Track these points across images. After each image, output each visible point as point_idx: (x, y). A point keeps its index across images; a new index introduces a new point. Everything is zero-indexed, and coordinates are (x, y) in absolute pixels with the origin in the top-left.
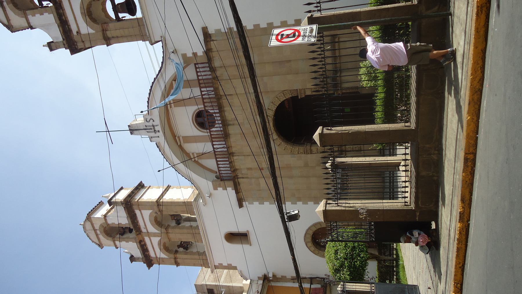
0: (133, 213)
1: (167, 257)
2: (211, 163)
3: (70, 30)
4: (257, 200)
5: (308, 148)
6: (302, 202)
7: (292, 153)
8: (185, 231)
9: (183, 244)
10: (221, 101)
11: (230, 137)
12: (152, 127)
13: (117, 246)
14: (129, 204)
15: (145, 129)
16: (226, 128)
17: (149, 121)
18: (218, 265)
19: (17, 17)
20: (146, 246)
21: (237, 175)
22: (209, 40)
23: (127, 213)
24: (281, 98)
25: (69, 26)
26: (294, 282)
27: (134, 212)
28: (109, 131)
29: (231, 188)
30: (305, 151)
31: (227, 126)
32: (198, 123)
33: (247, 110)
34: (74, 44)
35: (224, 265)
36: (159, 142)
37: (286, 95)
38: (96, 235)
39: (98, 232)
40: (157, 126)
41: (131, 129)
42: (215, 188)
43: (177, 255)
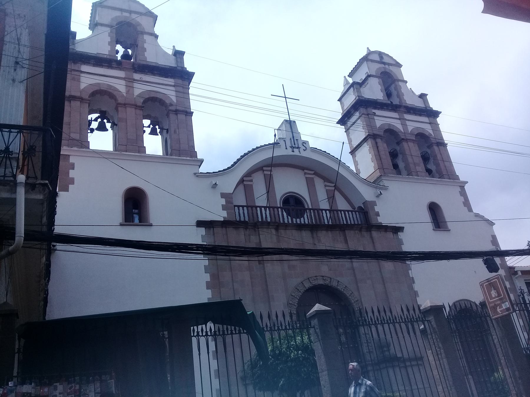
0: (170, 74)
2: (240, 200)
3: (375, 108)
9: (102, 120)
15: (293, 137)
17: (304, 146)
23: (166, 67)
25: (378, 109)
27: (172, 77)
28: (285, 98)
29: (226, 216)
32: (288, 198)
35: (71, 171)
37: (356, 303)
39: (126, 14)
42: (223, 195)
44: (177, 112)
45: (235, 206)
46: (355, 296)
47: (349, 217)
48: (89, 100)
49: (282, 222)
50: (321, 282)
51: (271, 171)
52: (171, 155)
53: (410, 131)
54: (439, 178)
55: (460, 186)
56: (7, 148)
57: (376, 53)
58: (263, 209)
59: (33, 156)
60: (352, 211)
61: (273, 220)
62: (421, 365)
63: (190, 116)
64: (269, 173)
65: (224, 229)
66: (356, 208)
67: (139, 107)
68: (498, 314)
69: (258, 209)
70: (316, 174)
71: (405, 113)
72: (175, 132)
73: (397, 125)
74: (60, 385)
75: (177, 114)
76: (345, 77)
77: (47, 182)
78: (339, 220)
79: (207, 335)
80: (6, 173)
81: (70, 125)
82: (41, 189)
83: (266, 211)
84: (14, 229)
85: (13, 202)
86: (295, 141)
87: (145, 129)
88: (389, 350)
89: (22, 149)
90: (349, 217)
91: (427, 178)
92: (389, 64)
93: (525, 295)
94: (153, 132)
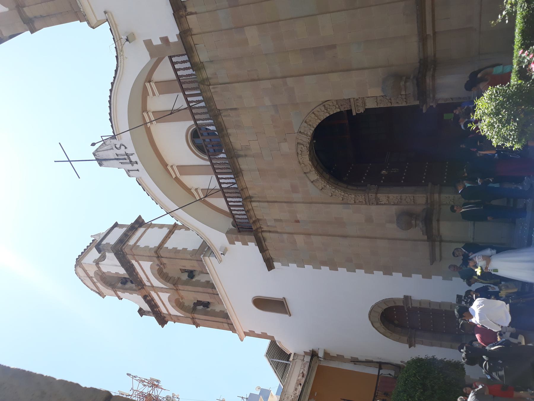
1: (183, 316)
4: (294, 262)
5: (371, 196)
6: (363, 271)
7: (345, 203)
8: (200, 289)
10: (220, 120)
12: (126, 157)
13: (120, 296)
14: (121, 253)
20: (155, 301)
21: (261, 228)
22: (184, 13)
26: (355, 364)
27: (129, 262)
30: (367, 200)
31: (235, 160)
33: (264, 133)
36: (140, 178)
37: (329, 110)
38: (93, 283)
39: (95, 280)
40: (132, 154)
41: (98, 158)
42: (232, 242)
43: (195, 315)
46: (319, 111)
50: (306, 158)
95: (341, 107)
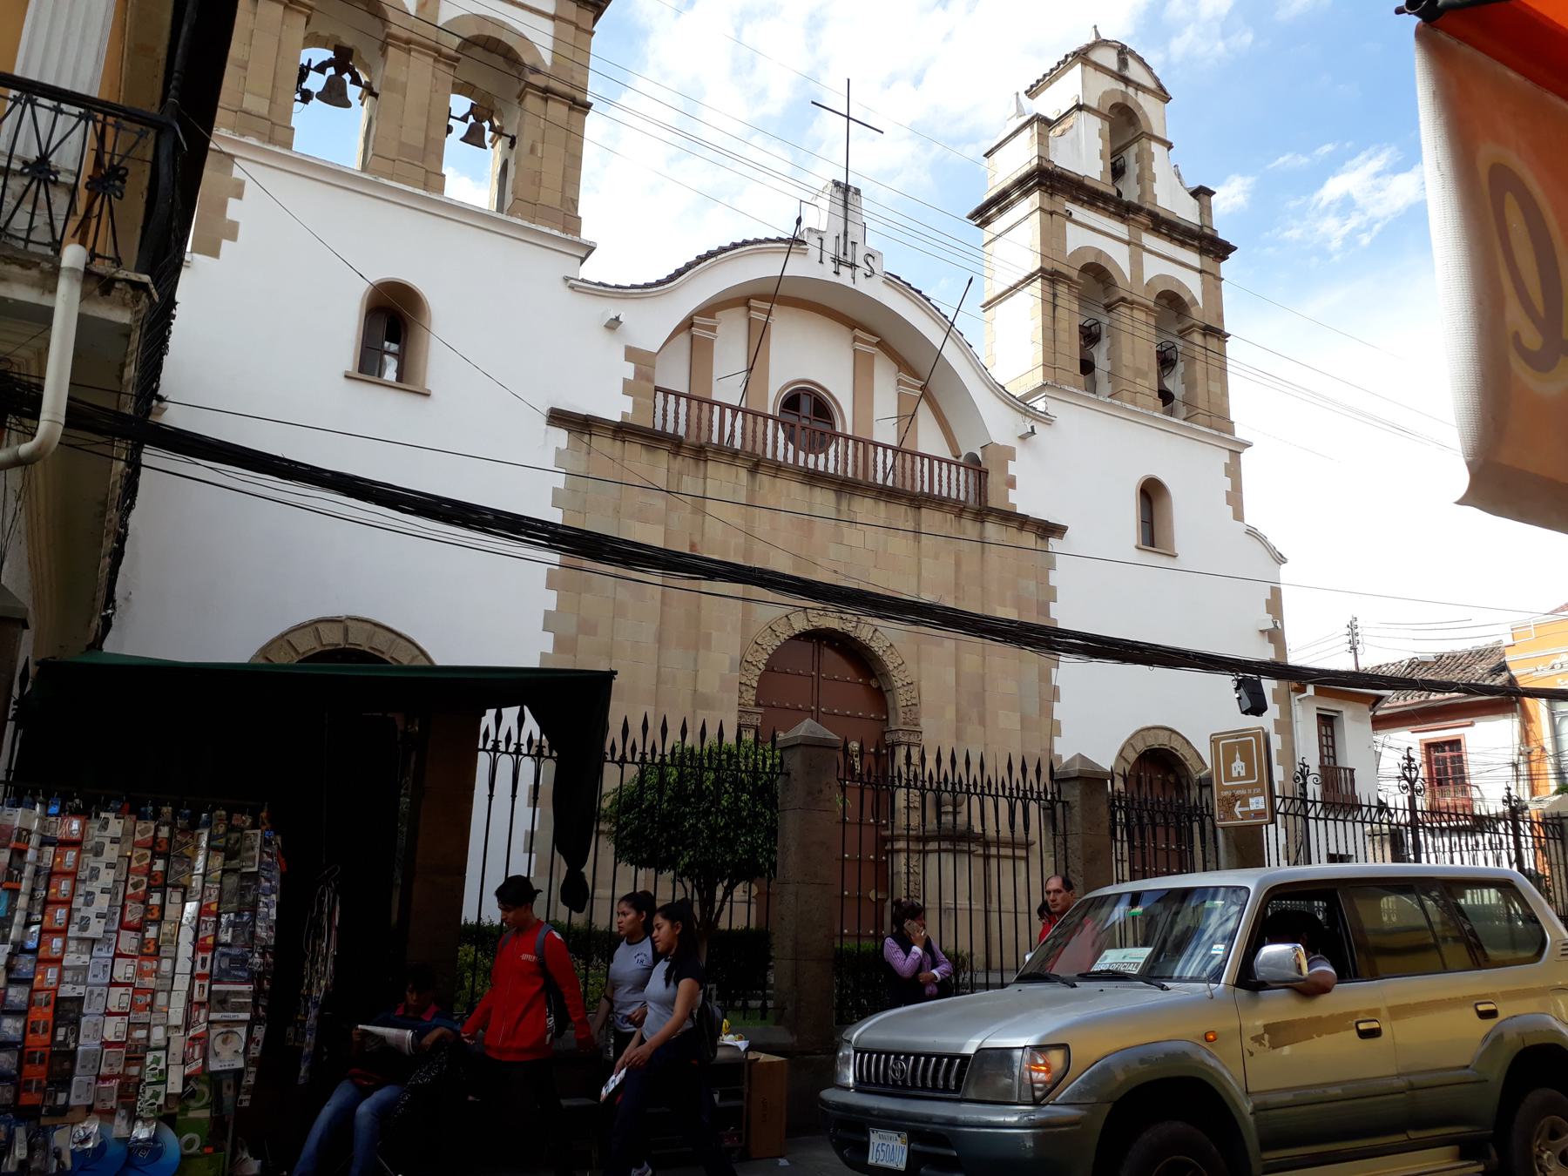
3: (1075, 200)
7: (744, 663)
9: (339, 72)
11: (804, 486)
16: (833, 483)
17: (868, 263)
18: (237, 173)
19: (1100, 94)
24: (902, 676)
25: (1083, 203)
29: (629, 410)
34: (1048, 187)
35: (232, 203)
37: (906, 689)
42: (632, 354)
44: (547, 93)
45: (657, 389)
47: (940, 476)
48: (311, 8)
49: (769, 456)
51: (769, 313)
52: (511, 213)
53: (1145, 282)
54: (1185, 419)
55: (1230, 450)
56: (44, 158)
57: (1114, 47)
58: (728, 412)
59: (117, 197)
60: (949, 463)
61: (749, 449)
62: (1021, 858)
63: (580, 111)
64: (763, 317)
65: (619, 443)
66: (964, 454)
67: (448, 57)
68: (1234, 817)
69: (717, 409)
70: (883, 345)
71: (1147, 230)
72: (533, 150)
73: (1119, 256)
74: (116, 818)
75: (546, 100)
76: (1017, 94)
77: (146, 278)
78: (913, 479)
79: (518, 751)
80: (34, 225)
81: (246, 69)
82: (128, 296)
83: (734, 417)
84: (40, 388)
85: (46, 315)
86: (849, 245)
87: (452, 122)
88: (955, 813)
89: (88, 169)
90: (940, 476)
91: (1156, 414)
92: (1139, 87)
93: (1310, 779)
94: (474, 137)
95: (906, 709)
